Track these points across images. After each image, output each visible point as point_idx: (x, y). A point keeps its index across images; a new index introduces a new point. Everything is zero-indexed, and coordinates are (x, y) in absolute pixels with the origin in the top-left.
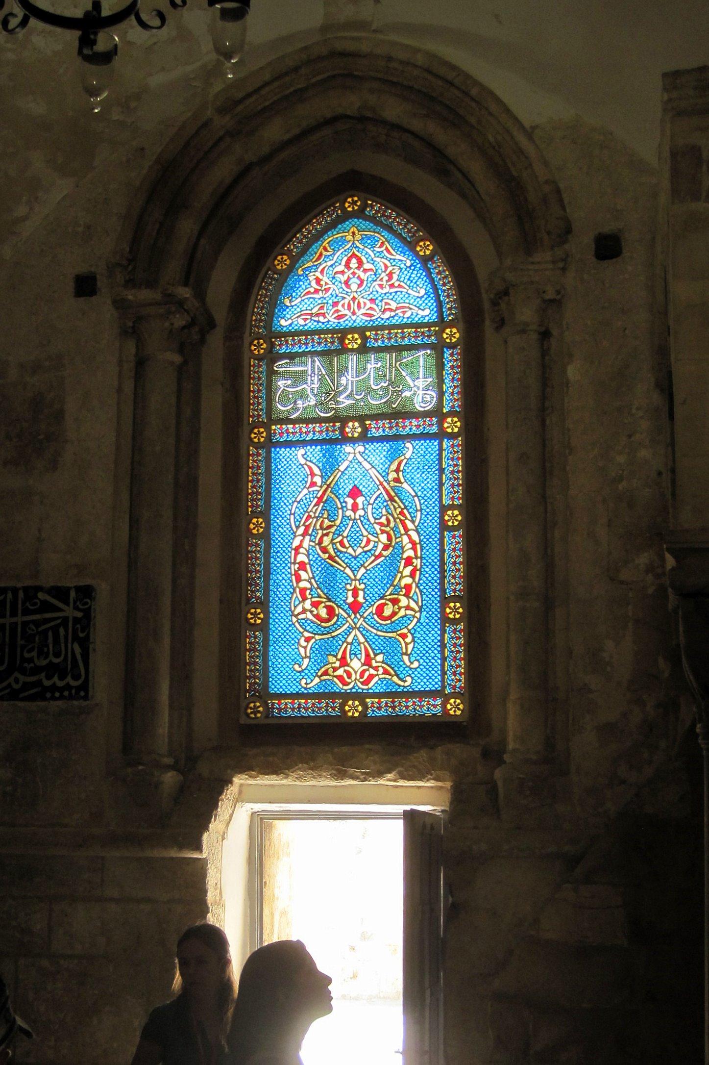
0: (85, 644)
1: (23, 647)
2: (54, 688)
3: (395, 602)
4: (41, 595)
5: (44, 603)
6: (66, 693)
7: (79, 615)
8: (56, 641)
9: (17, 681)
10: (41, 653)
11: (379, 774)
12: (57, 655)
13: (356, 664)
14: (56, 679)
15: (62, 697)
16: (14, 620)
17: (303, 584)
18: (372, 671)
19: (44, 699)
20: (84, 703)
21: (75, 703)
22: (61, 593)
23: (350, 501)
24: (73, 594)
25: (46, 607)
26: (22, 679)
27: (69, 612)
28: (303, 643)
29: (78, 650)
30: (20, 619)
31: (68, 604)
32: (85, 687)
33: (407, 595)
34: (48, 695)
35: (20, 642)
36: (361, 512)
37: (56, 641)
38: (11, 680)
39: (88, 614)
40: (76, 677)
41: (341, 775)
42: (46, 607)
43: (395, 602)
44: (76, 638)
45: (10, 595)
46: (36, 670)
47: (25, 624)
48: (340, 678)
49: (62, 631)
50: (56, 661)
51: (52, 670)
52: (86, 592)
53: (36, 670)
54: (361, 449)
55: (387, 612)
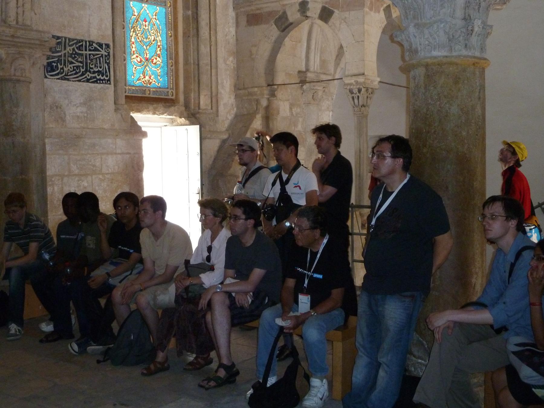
0: (108, 64)
1: (90, 63)
2: (100, 80)
3: (156, 59)
4: (94, 44)
5: (95, 48)
6: (104, 82)
7: (107, 54)
8: (100, 63)
9: (88, 75)
10: (95, 66)
11: (163, 114)
12: (101, 68)
13: (147, 78)
14: (100, 76)
15: (103, 83)
16: (86, 52)
17: (134, 49)
18: (151, 81)
19: (97, 83)
20: (109, 85)
21: (107, 85)
22: (100, 45)
23: (144, 23)
24: (104, 46)
25: (96, 50)
26: (90, 75)
27: (103, 52)
28: (134, 69)
29: (107, 67)
30: (88, 52)
31: (102, 49)
32: (109, 80)
33: (159, 57)
34: (99, 82)
35: (89, 61)
36: (147, 27)
37: (100, 63)
38: (86, 75)
39: (109, 55)
40: (107, 76)
41: (154, 113)
42: (96, 50)
43: (156, 59)
44: (106, 62)
45: (84, 43)
46: (94, 72)
47: (90, 55)
48: (144, 82)
49: (101, 58)
50: (100, 70)
51: (99, 72)
52: (108, 46)
53: (94, 72)
54: (146, 6)
55: (155, 61)
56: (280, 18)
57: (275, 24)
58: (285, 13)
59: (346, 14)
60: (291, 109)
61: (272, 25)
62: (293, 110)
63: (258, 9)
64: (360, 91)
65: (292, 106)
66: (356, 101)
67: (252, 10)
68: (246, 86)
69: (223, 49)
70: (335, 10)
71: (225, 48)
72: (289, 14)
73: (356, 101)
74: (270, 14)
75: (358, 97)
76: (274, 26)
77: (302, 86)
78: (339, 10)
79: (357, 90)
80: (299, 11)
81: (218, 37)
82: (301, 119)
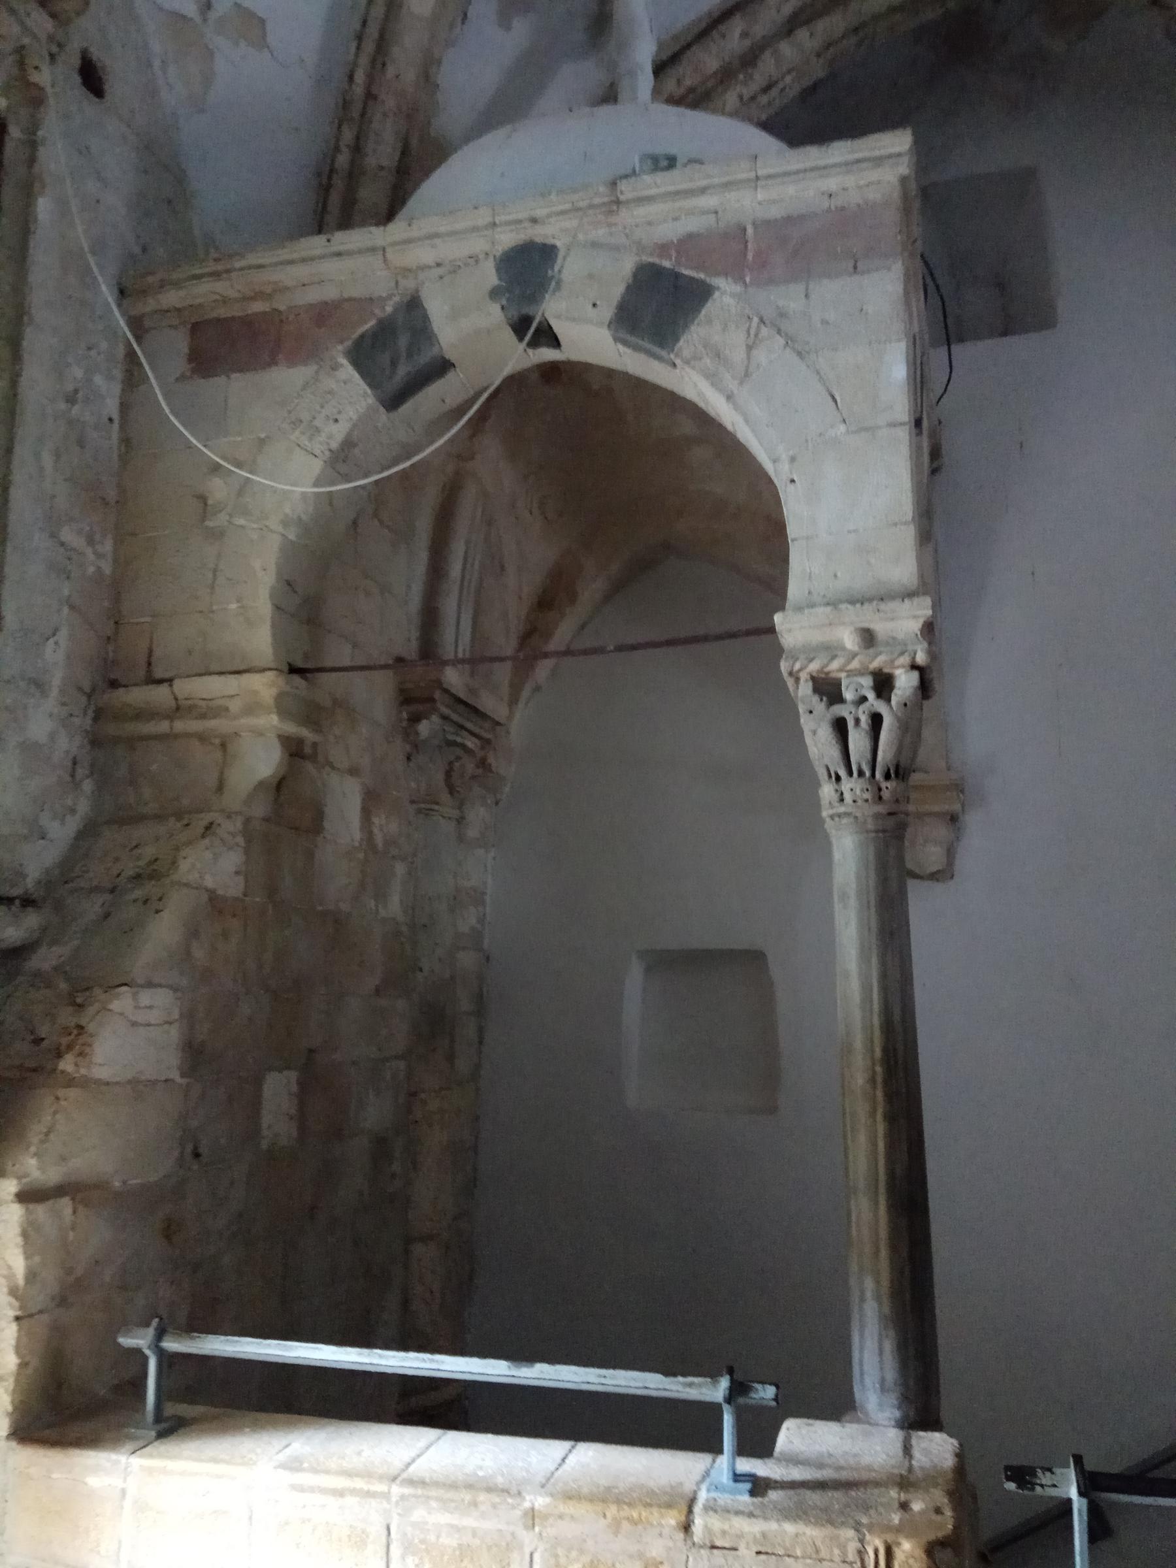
56: (385, 332)
57: (357, 364)
58: (414, 304)
59: (790, 298)
60: (366, 814)
61: (335, 367)
62: (376, 820)
63: (258, 296)
64: (883, 684)
65: (372, 800)
66: (858, 741)
67: (225, 301)
68: (159, 673)
69: (48, 460)
70: (720, 282)
71: (57, 455)
72: (436, 308)
73: (858, 741)
74: (325, 315)
75: (876, 720)
76: (348, 371)
77: (415, 719)
78: (740, 279)
79: (867, 681)
80: (494, 294)
81: (24, 381)
82: (400, 869)
